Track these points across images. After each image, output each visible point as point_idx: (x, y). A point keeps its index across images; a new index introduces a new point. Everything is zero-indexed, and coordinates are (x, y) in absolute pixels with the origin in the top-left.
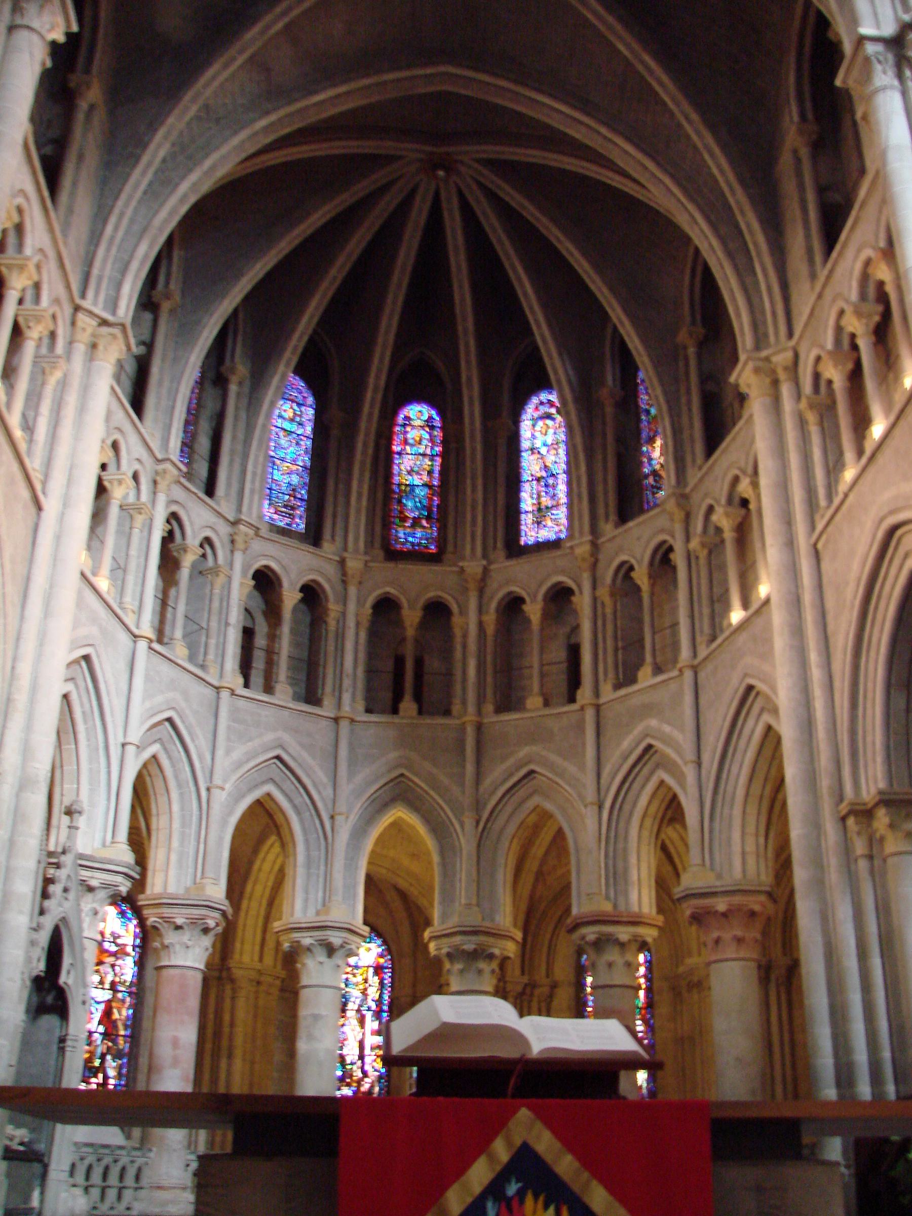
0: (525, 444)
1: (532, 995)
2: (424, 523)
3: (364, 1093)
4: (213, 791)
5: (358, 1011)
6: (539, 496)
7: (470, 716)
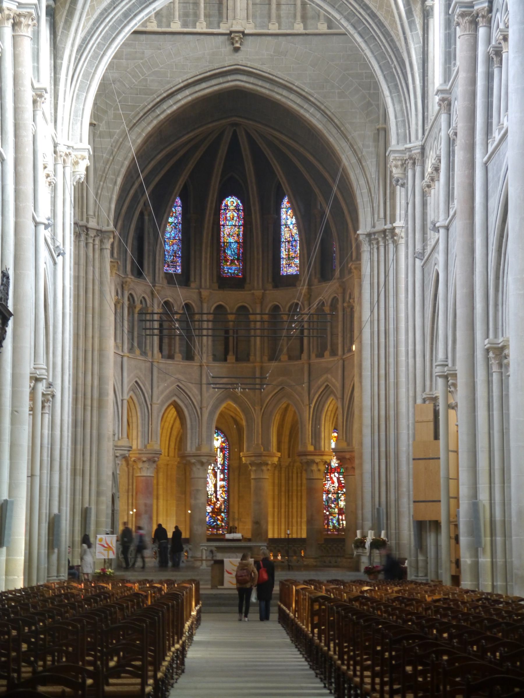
0: (283, 222)
1: (293, 466)
3: (217, 509)
4: (153, 405)
5: (213, 470)
6: (289, 251)
7: (258, 365)
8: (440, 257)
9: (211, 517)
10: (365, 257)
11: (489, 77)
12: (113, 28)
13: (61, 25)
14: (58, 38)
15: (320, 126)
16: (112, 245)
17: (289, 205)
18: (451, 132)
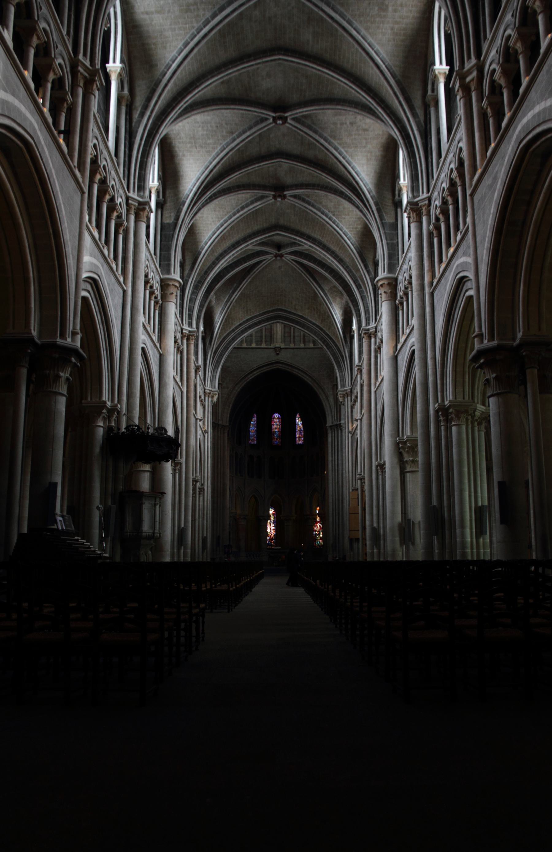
0: (297, 423)
2: (278, 439)
5: (270, 523)
6: (299, 435)
8: (358, 432)
9: (269, 542)
10: (330, 435)
11: (376, 357)
12: (228, 344)
13: (208, 343)
14: (207, 348)
15: (310, 383)
16: (228, 431)
17: (299, 416)
18: (362, 381)
